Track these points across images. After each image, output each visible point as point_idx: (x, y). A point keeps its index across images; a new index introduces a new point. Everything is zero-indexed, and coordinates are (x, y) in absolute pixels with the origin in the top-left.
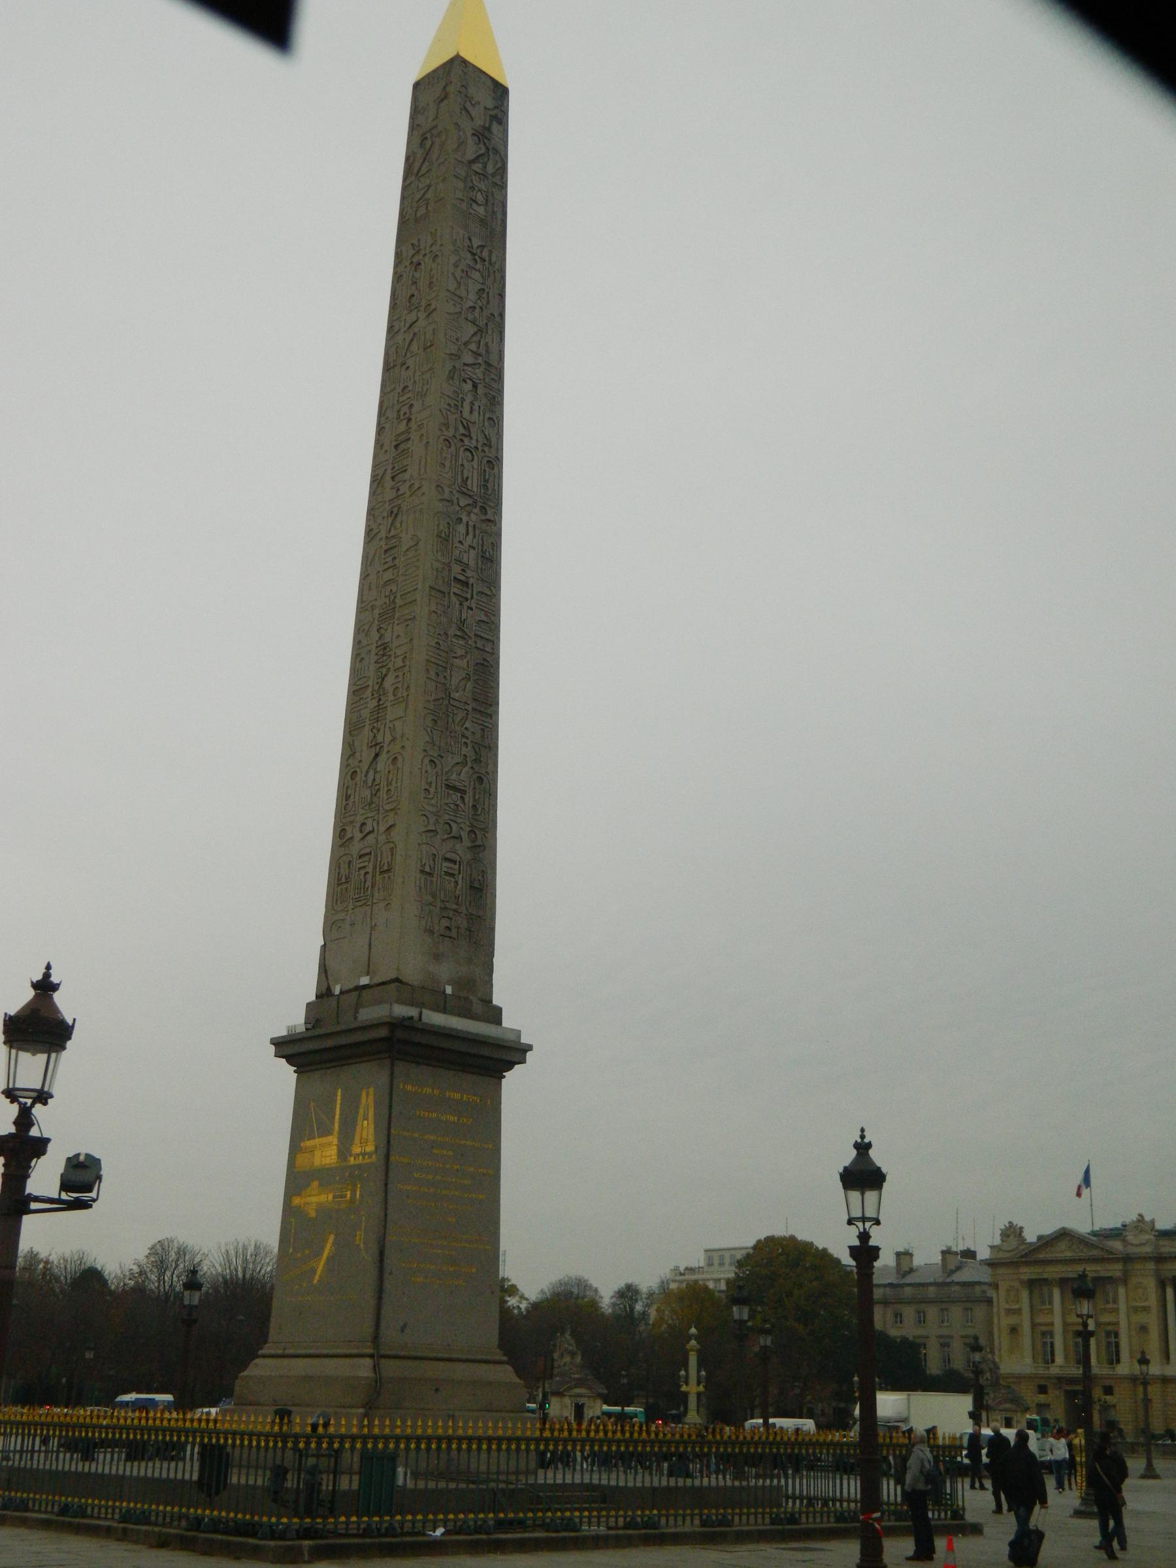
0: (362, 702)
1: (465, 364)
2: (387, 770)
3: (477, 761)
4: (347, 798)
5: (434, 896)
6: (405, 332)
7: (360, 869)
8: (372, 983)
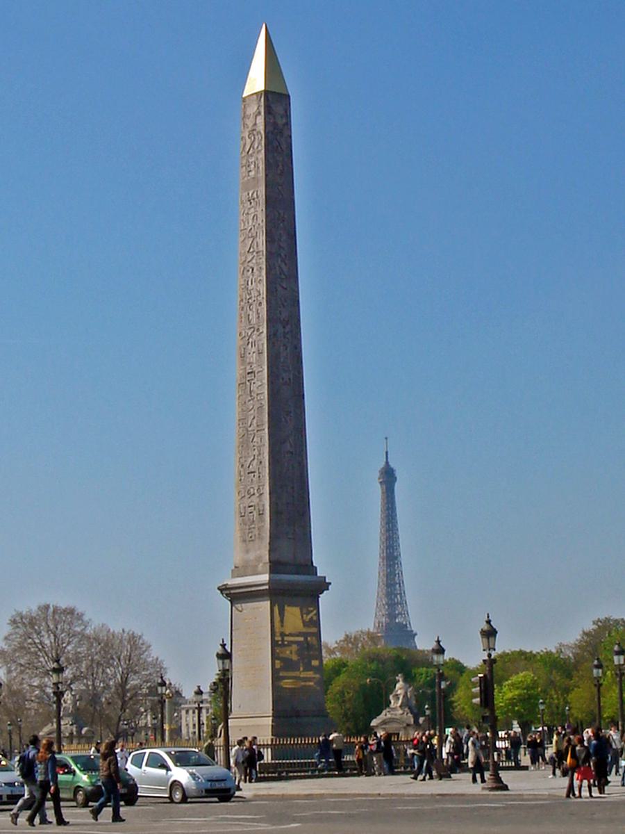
1: (249, 262)
3: (260, 454)
5: (246, 525)
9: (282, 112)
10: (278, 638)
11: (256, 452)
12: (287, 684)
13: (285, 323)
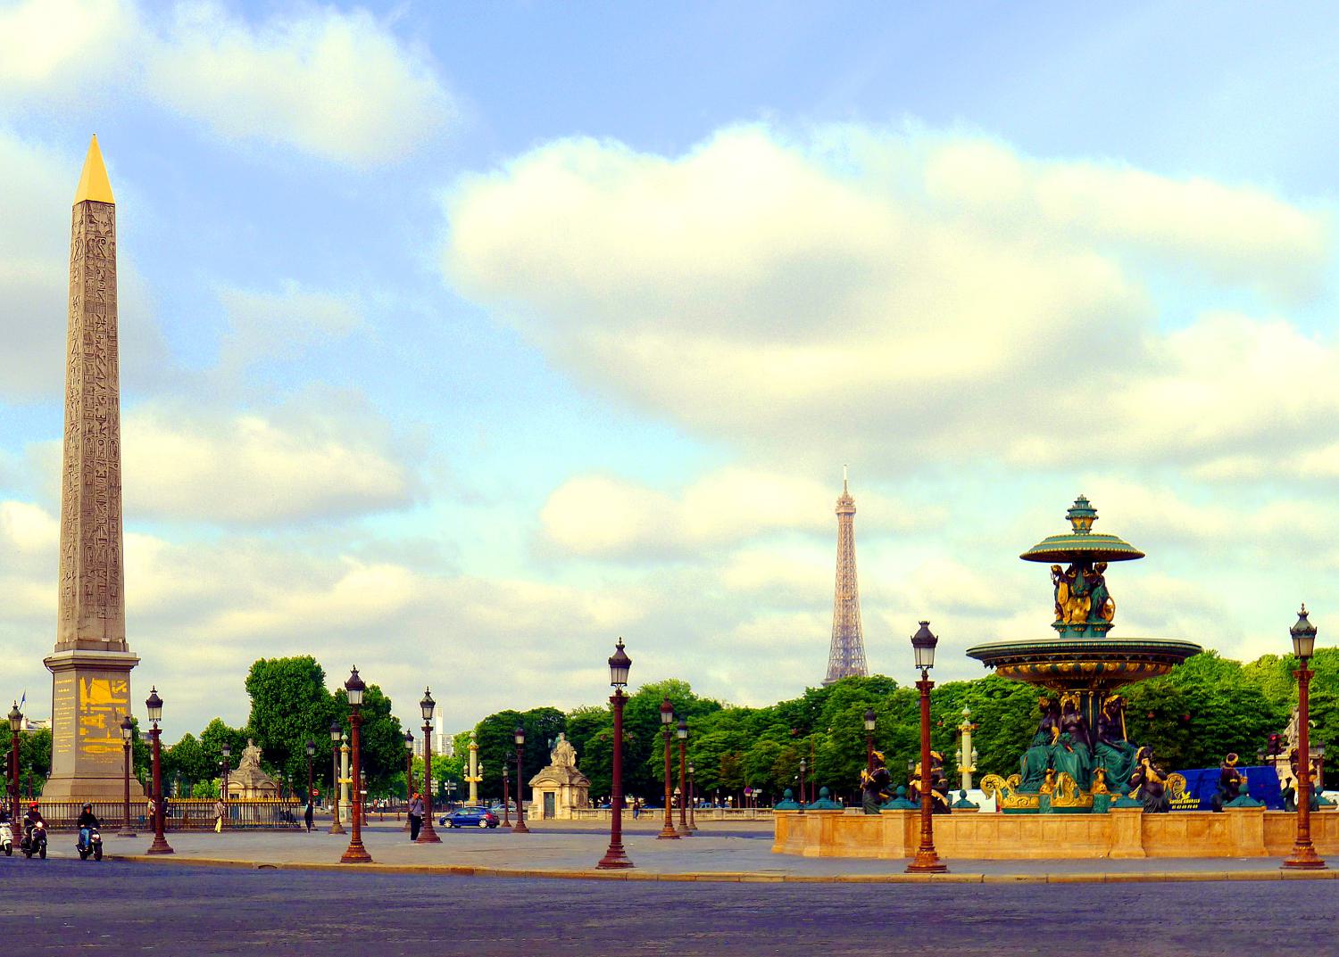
9: (105, 220)
10: (84, 708)
11: (72, 539)
12: (95, 749)
13: (102, 420)
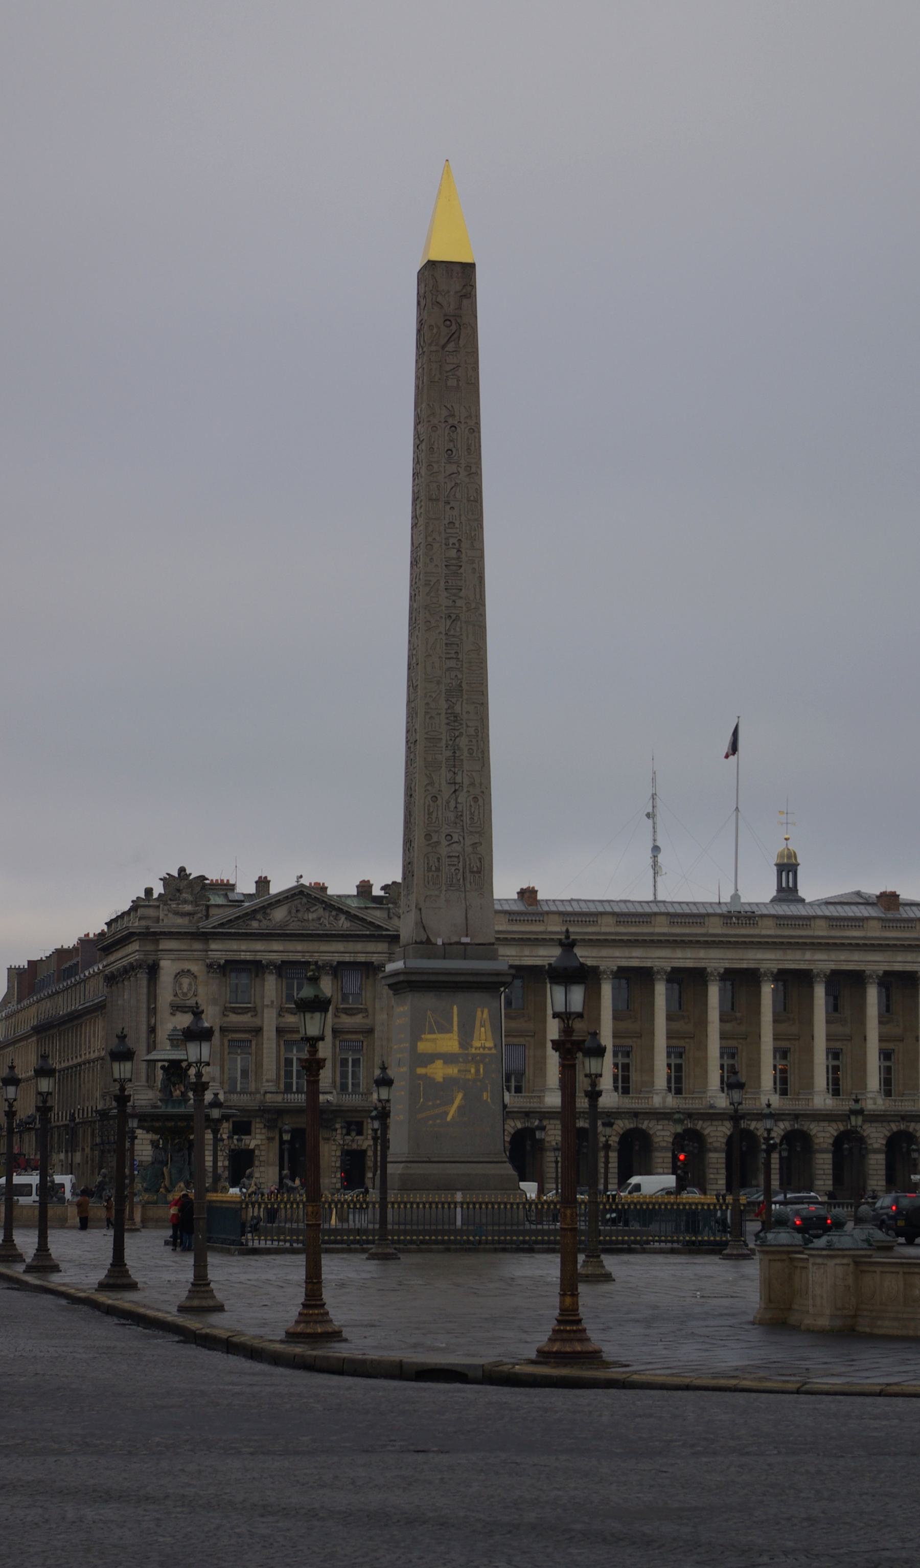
0: (436, 749)
2: (468, 804)
4: (430, 814)
6: (445, 477)
7: (449, 865)
8: (473, 942)
